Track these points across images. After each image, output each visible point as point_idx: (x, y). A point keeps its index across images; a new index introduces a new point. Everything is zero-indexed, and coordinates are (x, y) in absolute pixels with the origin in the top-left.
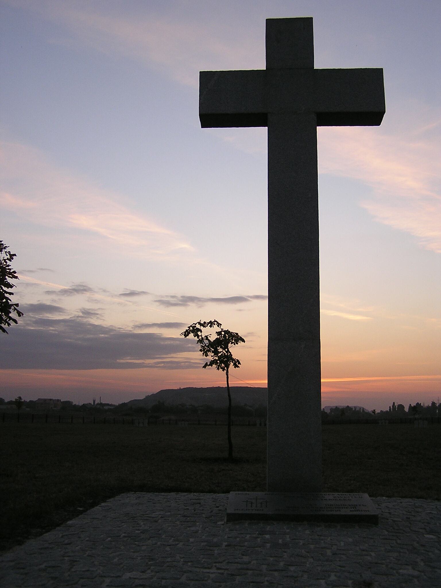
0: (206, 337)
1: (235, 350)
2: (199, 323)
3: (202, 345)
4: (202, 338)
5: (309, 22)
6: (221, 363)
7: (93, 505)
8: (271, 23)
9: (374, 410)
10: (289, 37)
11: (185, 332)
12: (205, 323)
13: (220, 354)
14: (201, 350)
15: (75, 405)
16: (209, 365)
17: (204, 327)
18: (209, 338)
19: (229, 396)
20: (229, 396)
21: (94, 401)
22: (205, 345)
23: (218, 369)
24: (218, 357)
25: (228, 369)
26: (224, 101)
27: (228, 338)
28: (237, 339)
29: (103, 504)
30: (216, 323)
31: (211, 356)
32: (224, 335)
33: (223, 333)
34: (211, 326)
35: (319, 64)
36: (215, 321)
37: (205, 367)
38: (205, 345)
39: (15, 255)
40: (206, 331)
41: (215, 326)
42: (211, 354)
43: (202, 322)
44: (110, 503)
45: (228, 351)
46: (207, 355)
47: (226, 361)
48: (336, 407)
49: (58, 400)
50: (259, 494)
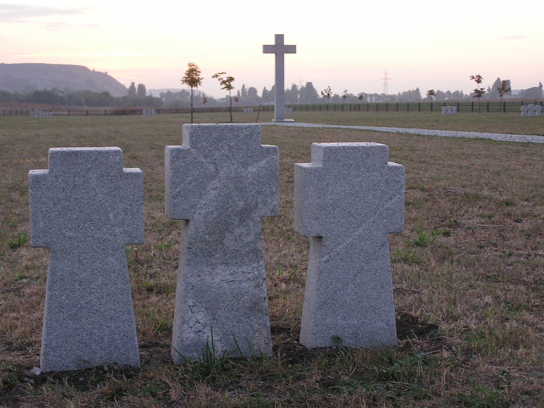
1: (232, 84)
10: (279, 38)
26: (267, 49)
31: (224, 86)
40: (221, 76)
48: (169, 91)
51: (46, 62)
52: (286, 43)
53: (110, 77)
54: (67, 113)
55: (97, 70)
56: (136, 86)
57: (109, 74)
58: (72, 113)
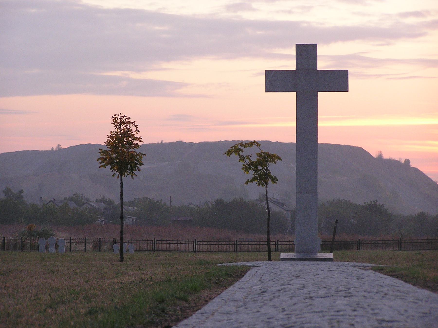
6: (261, 179)
8: (297, 45)
10: (306, 53)
12: (246, 144)
13: (259, 172)
14: (243, 169)
18: (250, 158)
22: (247, 164)
23: (259, 185)
24: (258, 175)
25: (267, 185)
26: (276, 81)
31: (251, 174)
32: (264, 157)
33: (263, 154)
38: (247, 164)
39: (138, 126)
40: (246, 152)
45: (267, 169)
51: (273, 140)
53: (416, 170)
54: (191, 247)
55: (386, 156)
57: (413, 164)
58: (200, 247)
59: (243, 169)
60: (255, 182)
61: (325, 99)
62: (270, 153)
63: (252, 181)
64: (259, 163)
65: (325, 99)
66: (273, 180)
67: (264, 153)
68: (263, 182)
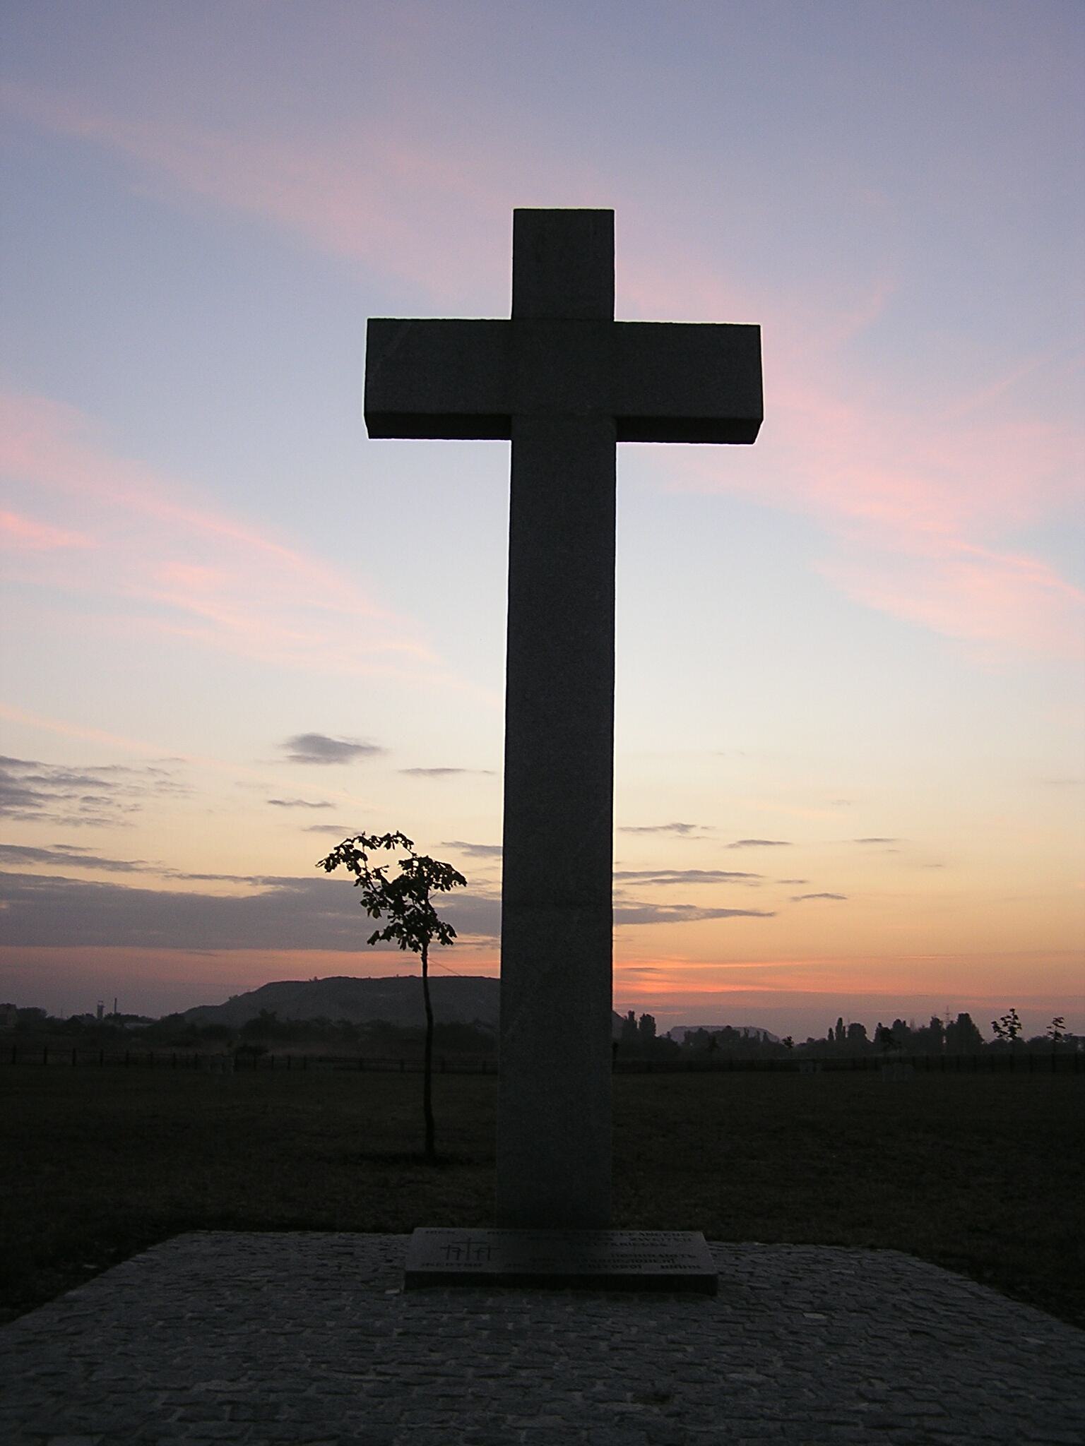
0: (377, 871)
2: (362, 839)
3: (366, 889)
4: (368, 874)
5: (604, 219)
6: (409, 933)
7: (118, 1258)
9: (790, 1038)
10: (564, 251)
11: (328, 860)
12: (374, 838)
13: (407, 913)
14: (364, 903)
15: (52, 1019)
16: (383, 938)
17: (372, 847)
18: (383, 874)
19: (428, 1010)
20: (428, 1010)
21: (100, 1009)
22: (375, 891)
24: (404, 918)
27: (428, 874)
28: (449, 876)
29: (139, 1256)
30: (399, 839)
31: (386, 919)
32: (419, 868)
33: (416, 863)
34: (388, 846)
35: (627, 309)
36: (399, 835)
37: (372, 941)
38: (375, 891)
40: (376, 859)
41: (399, 846)
42: (386, 913)
43: (367, 838)
44: (157, 1253)
46: (377, 915)
47: (420, 928)
48: (701, 1029)
49: (9, 1006)
50: (476, 1233)
52: (646, 292)
56: (637, 1018)
59: (364, 903)
60: (394, 939)
61: (649, 476)
62: (434, 860)
63: (388, 935)
64: (402, 885)
65: (649, 476)
66: (442, 936)
67: (420, 860)
68: (415, 938)
